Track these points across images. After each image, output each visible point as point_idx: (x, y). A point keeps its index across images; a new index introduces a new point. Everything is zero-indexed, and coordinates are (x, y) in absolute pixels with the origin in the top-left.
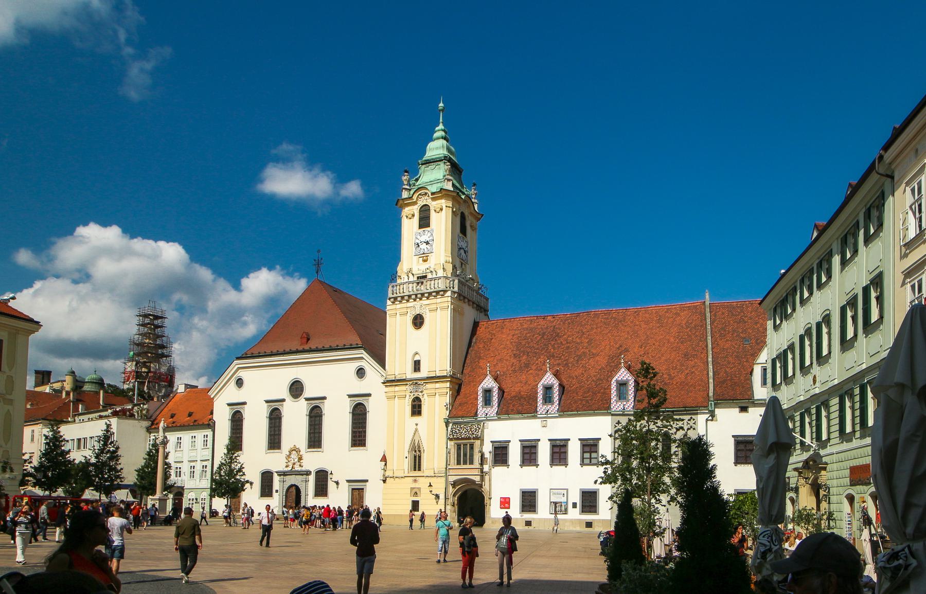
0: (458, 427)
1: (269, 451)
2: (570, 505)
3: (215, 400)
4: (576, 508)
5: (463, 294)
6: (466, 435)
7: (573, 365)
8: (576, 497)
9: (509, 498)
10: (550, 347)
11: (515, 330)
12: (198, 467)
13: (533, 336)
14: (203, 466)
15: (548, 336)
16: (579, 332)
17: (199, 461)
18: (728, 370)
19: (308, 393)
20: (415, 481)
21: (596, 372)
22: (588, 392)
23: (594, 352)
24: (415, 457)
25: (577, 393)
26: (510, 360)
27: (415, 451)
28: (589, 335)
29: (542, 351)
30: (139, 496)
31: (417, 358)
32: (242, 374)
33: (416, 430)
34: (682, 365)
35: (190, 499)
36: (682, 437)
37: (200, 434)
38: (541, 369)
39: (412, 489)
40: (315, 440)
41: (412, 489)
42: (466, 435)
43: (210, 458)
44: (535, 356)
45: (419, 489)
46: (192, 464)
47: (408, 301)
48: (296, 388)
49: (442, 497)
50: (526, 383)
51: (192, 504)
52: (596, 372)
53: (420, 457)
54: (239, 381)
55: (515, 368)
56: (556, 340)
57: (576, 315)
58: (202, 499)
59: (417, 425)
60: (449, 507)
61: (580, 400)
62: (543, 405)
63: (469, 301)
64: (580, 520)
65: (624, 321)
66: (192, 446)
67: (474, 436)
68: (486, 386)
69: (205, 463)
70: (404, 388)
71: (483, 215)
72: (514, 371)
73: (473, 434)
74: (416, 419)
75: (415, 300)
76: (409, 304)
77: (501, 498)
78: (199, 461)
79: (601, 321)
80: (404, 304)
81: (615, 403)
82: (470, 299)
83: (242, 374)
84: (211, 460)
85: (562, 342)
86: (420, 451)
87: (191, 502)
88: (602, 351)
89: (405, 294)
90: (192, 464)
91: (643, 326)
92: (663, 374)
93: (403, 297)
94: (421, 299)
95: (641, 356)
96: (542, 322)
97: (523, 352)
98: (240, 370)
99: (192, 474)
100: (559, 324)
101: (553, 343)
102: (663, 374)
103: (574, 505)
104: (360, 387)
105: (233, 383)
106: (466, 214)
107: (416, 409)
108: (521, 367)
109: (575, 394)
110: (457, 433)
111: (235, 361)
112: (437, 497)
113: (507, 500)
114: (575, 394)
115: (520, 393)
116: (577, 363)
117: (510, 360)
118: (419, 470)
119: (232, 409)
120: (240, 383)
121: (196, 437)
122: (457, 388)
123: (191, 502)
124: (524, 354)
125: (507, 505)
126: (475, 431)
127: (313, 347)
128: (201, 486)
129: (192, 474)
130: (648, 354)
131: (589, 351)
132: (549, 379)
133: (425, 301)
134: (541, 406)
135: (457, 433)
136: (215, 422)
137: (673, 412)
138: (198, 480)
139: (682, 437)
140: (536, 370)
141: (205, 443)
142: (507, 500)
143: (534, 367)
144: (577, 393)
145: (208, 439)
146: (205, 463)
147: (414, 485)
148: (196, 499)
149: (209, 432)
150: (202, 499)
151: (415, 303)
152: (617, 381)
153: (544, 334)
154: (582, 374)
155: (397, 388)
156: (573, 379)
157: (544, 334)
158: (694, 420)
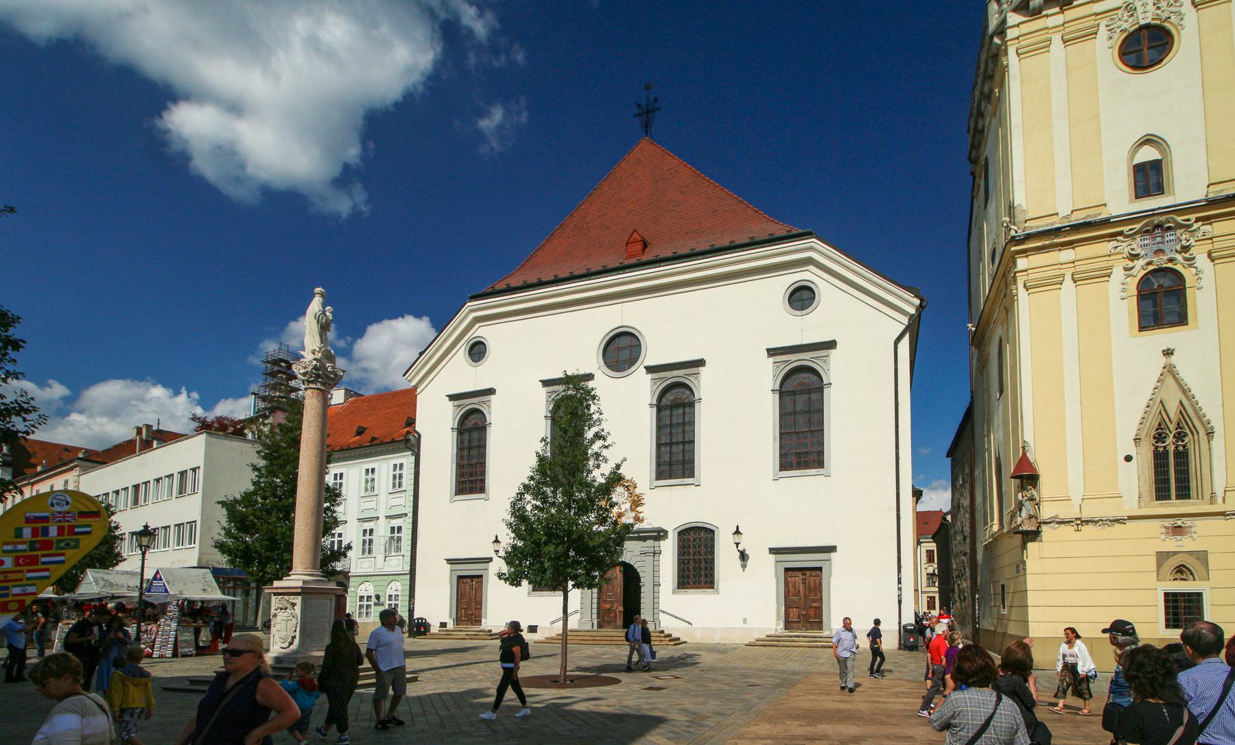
3: (419, 390)
12: (382, 530)
14: (393, 529)
17: (382, 519)
30: (255, 591)
32: (483, 332)
35: (362, 598)
37: (384, 466)
43: (409, 510)
46: (368, 526)
51: (368, 607)
54: (476, 349)
58: (390, 596)
66: (366, 490)
69: (396, 523)
78: (382, 519)
83: (483, 332)
84: (410, 515)
87: (365, 603)
90: (368, 526)
98: (478, 325)
99: (368, 547)
105: (461, 353)
111: (468, 304)
119: (459, 406)
120: (477, 351)
121: (376, 471)
123: (365, 603)
128: (388, 570)
129: (368, 547)
136: (419, 436)
138: (381, 557)
141: (397, 480)
145: (404, 472)
146: (396, 523)
148: (378, 597)
149: (407, 459)
150: (390, 596)
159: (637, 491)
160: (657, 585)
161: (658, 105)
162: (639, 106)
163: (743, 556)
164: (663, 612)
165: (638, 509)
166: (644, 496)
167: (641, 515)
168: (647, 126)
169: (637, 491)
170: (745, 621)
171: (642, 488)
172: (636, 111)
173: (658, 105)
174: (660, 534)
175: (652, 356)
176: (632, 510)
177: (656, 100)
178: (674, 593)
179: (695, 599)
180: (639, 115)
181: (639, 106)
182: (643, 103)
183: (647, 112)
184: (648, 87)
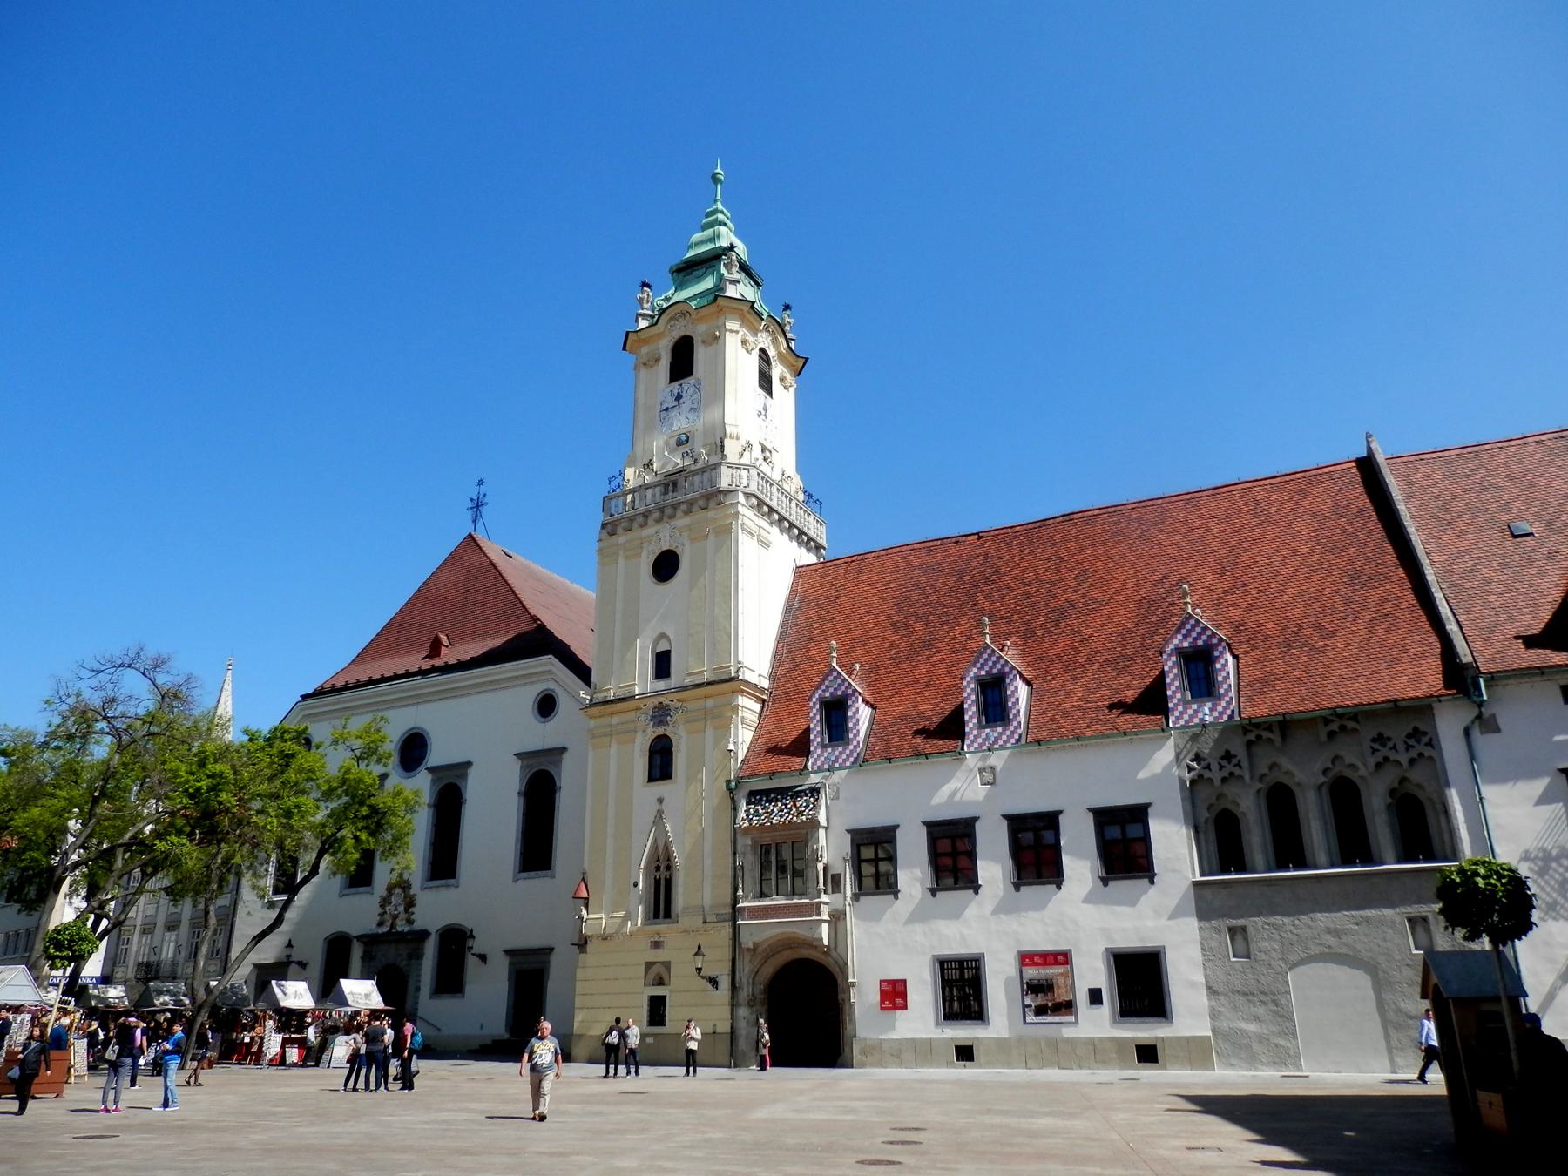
0: (761, 800)
1: (348, 891)
2: (1082, 999)
4: (1101, 1003)
5: (767, 500)
6: (781, 816)
7: (1047, 630)
8: (1092, 972)
9: (904, 982)
10: (981, 599)
11: (892, 572)
13: (937, 579)
15: (974, 576)
16: (1049, 559)
18: (1492, 598)
19: (437, 755)
20: (657, 945)
21: (1111, 641)
22: (1099, 687)
23: (1097, 595)
24: (657, 882)
25: (1067, 694)
26: (884, 637)
27: (658, 869)
28: (1077, 562)
29: (960, 609)
31: (662, 647)
33: (660, 814)
34: (1348, 603)
36: (1396, 785)
38: (965, 649)
39: (649, 965)
40: (443, 863)
41: (649, 965)
42: (781, 816)
44: (946, 623)
45: (667, 965)
47: (643, 526)
48: (413, 749)
49: (725, 983)
50: (928, 684)
52: (1111, 641)
53: (669, 882)
55: (897, 653)
56: (994, 582)
57: (1038, 524)
59: (661, 801)
60: (743, 1012)
61: (1080, 709)
62: (981, 727)
63: (782, 519)
64: (1119, 1043)
65: (1163, 523)
67: (804, 818)
68: (827, 694)
70: (632, 715)
71: (807, 359)
72: (897, 660)
73: (801, 813)
74: (661, 788)
75: (659, 521)
76: (649, 531)
77: (882, 982)
79: (1104, 529)
80: (637, 533)
81: (1180, 708)
82: (783, 512)
85: (1009, 587)
86: (668, 868)
88: (1117, 593)
89: (637, 511)
91: (1216, 527)
92: (1300, 628)
93: (631, 520)
94: (672, 517)
95: (1225, 592)
96: (954, 549)
97: (916, 615)
100: (998, 548)
101: (986, 589)
102: (1300, 628)
103: (1095, 997)
104: (541, 735)
106: (772, 353)
107: (661, 762)
108: (912, 649)
109: (1061, 698)
110: (759, 816)
112: (714, 981)
113: (899, 988)
114: (1061, 698)
115: (915, 707)
116: (1057, 626)
117: (884, 637)
118: (668, 915)
122: (758, 711)
124: (916, 621)
125: (898, 1001)
126: (807, 807)
127: (452, 661)
130: (1245, 585)
131: (1084, 596)
132: (990, 663)
133: (682, 521)
134: (975, 732)
135: (759, 816)
137: (1354, 717)
139: (1396, 785)
140: (953, 650)
142: (899, 988)
143: (945, 646)
144: (1067, 694)
147: (653, 956)
151: (658, 527)
152: (1179, 652)
153: (962, 572)
154: (1075, 648)
155: (615, 720)
156: (1052, 661)
157: (962, 572)
158: (1425, 733)
159: (412, 892)
160: (418, 989)
161: (486, 500)
162: (472, 500)
163: (483, 958)
164: (421, 1018)
165: (411, 910)
166: (416, 897)
167: (413, 917)
168: (475, 521)
169: (412, 892)
170: (482, 1027)
171: (415, 889)
172: (470, 504)
173: (486, 500)
174: (424, 935)
175: (436, 757)
176: (406, 910)
177: (484, 496)
178: (430, 998)
179: (447, 1004)
180: (471, 508)
181: (472, 500)
182: (476, 498)
183: (478, 506)
184: (480, 482)
